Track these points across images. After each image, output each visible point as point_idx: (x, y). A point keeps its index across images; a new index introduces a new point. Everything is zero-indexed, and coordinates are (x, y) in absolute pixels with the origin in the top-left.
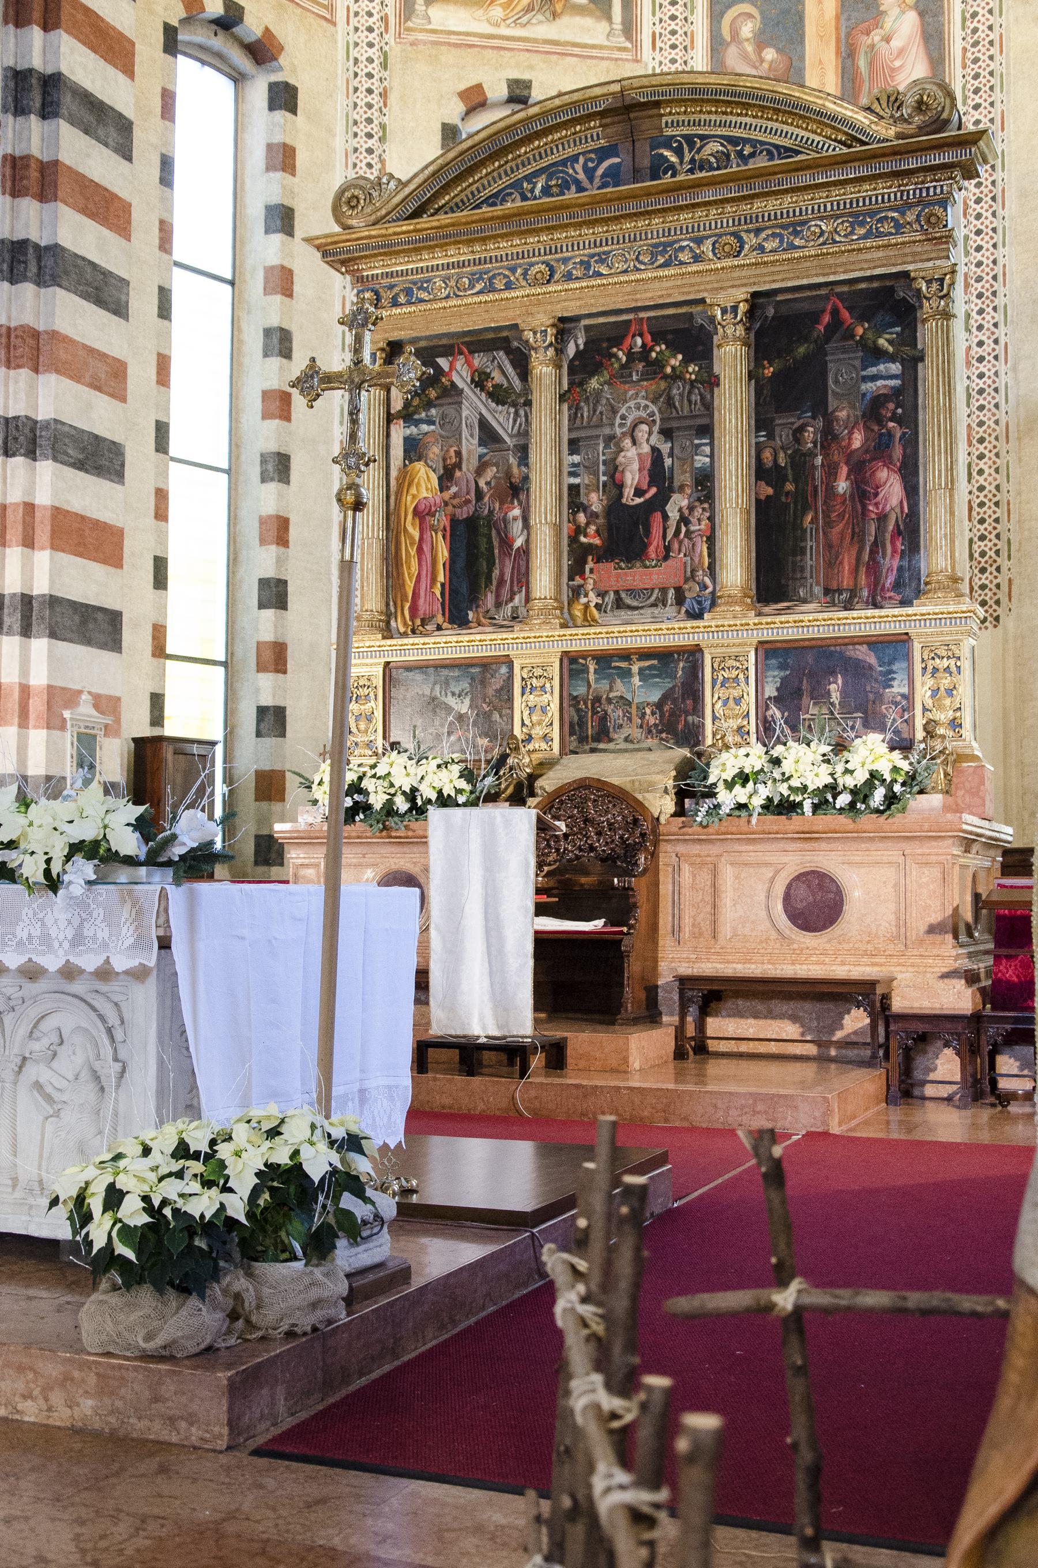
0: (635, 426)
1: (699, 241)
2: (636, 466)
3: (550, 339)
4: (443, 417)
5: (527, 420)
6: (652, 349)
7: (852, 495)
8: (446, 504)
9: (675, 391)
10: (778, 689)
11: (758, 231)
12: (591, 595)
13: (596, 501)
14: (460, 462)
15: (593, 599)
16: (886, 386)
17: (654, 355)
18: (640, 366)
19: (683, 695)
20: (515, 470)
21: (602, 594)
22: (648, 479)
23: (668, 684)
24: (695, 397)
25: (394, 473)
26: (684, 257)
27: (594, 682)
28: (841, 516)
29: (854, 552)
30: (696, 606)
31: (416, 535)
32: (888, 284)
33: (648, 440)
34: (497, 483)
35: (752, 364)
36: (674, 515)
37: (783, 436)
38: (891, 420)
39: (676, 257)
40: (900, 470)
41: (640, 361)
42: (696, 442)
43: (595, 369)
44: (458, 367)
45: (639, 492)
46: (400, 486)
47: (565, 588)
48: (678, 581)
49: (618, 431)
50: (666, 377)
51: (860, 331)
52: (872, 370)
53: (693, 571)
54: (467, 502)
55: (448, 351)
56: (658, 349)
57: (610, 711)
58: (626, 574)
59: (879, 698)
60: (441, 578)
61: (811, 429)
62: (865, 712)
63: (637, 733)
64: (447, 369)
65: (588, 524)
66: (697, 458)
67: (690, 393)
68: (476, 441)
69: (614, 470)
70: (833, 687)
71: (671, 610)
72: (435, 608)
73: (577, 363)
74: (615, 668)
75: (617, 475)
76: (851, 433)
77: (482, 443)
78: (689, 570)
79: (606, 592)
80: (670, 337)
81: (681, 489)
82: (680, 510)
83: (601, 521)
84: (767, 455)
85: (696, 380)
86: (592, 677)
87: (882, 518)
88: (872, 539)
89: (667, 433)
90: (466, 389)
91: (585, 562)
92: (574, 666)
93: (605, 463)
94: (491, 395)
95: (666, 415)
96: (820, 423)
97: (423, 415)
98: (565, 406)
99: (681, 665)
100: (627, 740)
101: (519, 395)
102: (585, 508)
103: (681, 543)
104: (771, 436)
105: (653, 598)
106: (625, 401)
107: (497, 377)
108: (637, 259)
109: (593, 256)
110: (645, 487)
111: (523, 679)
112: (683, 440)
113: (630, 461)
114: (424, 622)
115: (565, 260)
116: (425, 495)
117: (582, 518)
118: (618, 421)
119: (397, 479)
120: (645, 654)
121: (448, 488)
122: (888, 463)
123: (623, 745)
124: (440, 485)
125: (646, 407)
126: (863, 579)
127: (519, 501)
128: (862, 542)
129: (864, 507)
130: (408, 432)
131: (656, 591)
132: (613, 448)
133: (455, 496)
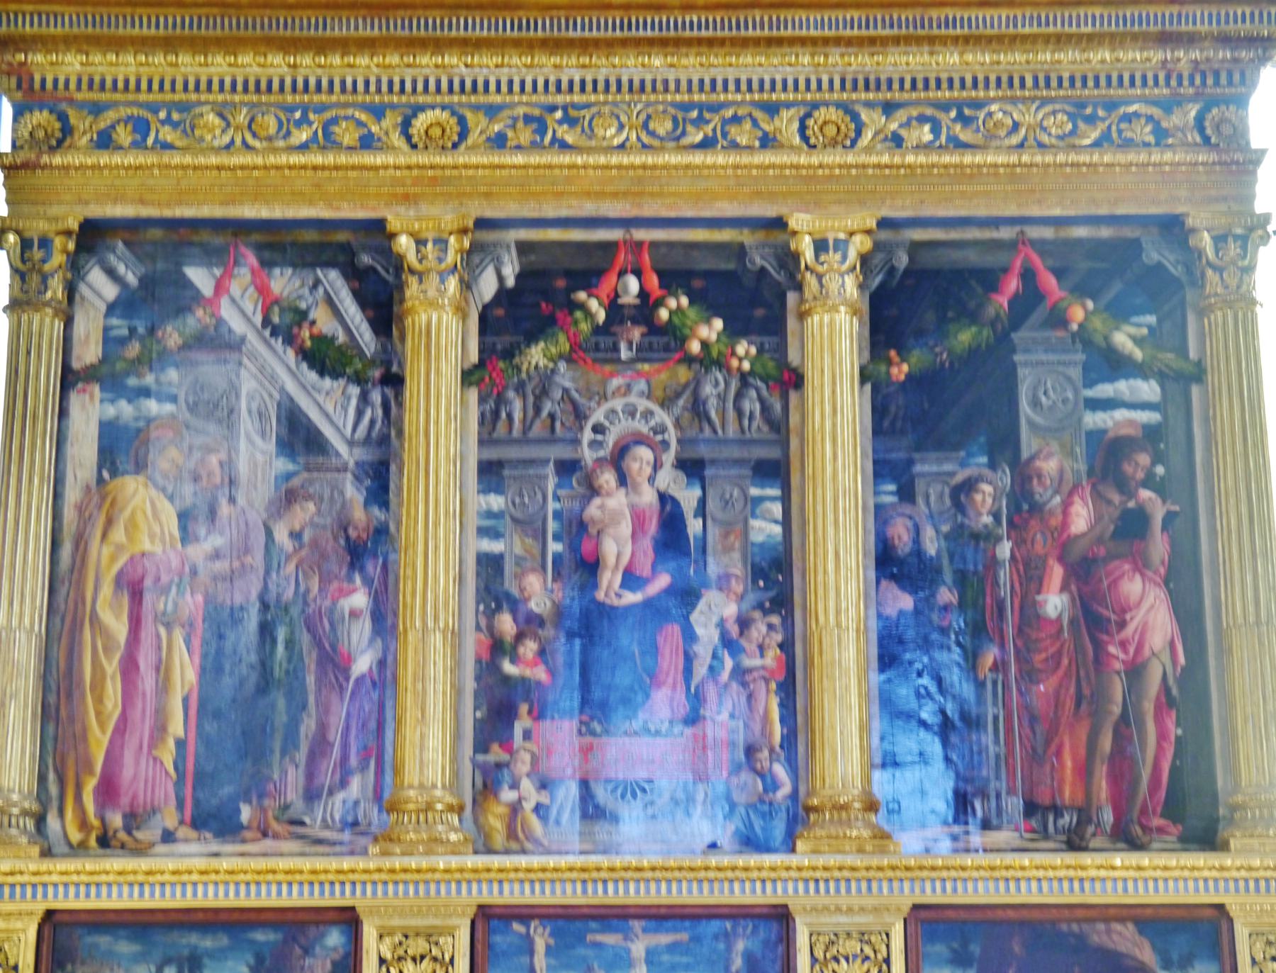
1: (772, 109)
2: (626, 528)
3: (451, 257)
6: (660, 303)
7: (1072, 621)
11: (889, 108)
12: (527, 785)
16: (1131, 423)
17: (664, 314)
18: (636, 333)
20: (359, 514)
24: (751, 404)
25: (72, 495)
26: (743, 135)
29: (1083, 733)
31: (119, 628)
32: (1129, 232)
33: (651, 480)
35: (867, 354)
39: (724, 135)
40: (1166, 583)
41: (635, 322)
42: (754, 491)
45: (631, 579)
47: (468, 766)
50: (689, 360)
51: (1077, 314)
52: (1105, 390)
55: (211, 256)
56: (672, 303)
60: (177, 727)
61: (987, 488)
65: (520, 637)
66: (755, 523)
67: (739, 396)
68: (271, 446)
72: (160, 794)
73: (500, 312)
76: (1067, 505)
80: (697, 284)
81: (723, 582)
82: (721, 624)
85: (752, 373)
87: (1135, 671)
88: (1117, 710)
89: (692, 468)
90: (252, 337)
93: (557, 515)
96: (1005, 478)
97: (149, 379)
98: (473, 395)
99: (740, 946)
102: (514, 604)
104: (907, 494)
106: (604, 397)
107: (324, 322)
108: (645, 126)
109: (552, 109)
113: (615, 518)
114: (133, 820)
115: (492, 111)
116: (147, 546)
117: (507, 624)
118: (588, 435)
119: (80, 509)
122: (1141, 565)
125: (648, 414)
126: (1102, 788)
128: (1097, 715)
129: (1099, 647)
130: (111, 411)
133: (216, 555)
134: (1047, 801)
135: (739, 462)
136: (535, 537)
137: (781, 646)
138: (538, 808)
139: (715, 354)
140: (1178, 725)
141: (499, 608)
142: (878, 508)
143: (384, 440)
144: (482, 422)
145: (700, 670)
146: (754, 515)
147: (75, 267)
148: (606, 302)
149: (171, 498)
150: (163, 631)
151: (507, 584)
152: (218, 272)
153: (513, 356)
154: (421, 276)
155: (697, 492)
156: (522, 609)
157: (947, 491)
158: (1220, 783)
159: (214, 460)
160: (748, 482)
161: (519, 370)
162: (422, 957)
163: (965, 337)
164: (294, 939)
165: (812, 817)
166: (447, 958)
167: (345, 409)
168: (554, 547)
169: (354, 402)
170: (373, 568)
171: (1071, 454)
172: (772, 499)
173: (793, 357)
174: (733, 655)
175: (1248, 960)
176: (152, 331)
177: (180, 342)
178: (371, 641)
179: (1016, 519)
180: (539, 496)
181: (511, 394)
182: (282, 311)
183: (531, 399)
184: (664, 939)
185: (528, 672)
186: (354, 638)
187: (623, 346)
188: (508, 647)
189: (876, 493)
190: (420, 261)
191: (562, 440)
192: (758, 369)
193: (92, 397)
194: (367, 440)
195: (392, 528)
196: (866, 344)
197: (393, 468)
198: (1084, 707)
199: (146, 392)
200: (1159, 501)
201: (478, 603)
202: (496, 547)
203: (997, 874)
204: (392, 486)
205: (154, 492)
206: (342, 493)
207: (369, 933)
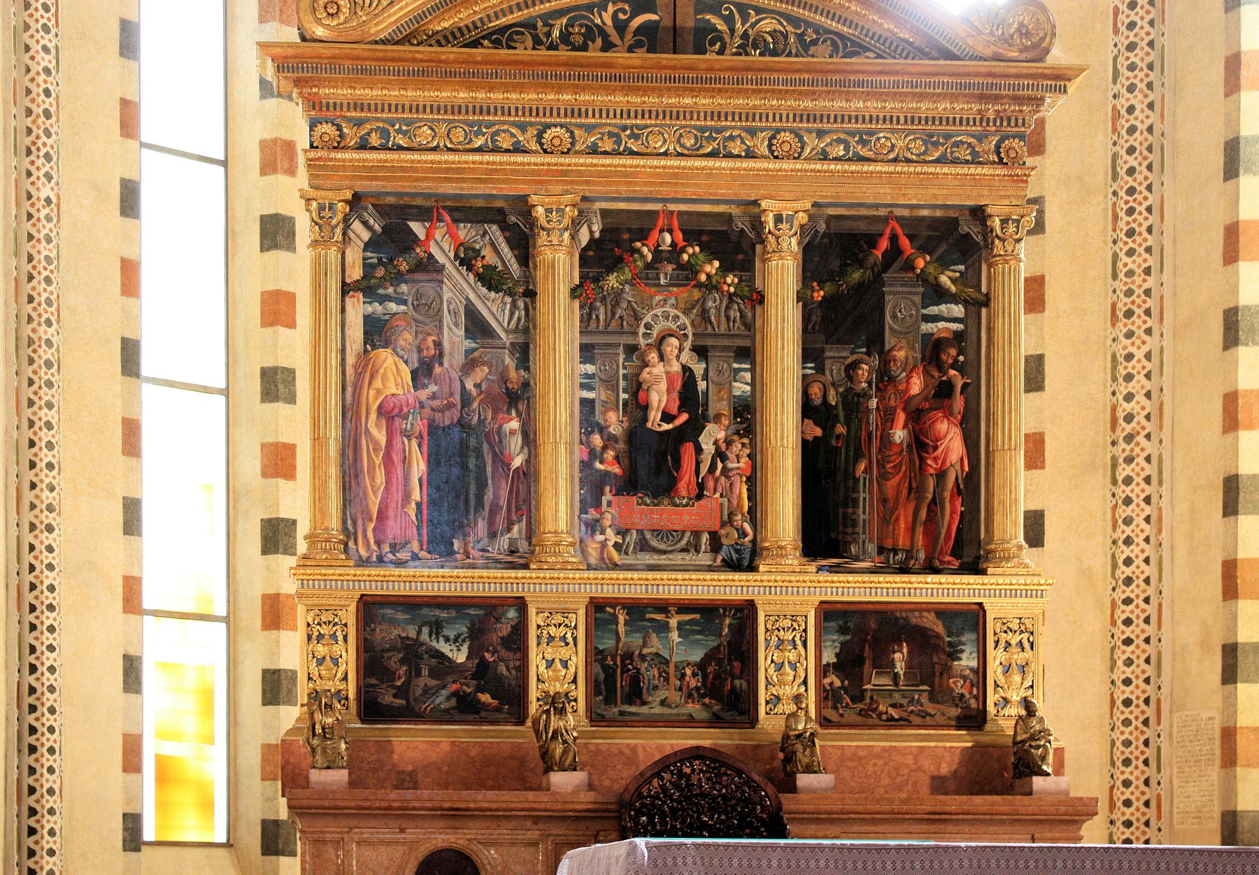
0: (662, 339)
2: (663, 386)
3: (567, 221)
4: (418, 296)
5: (527, 314)
8: (422, 406)
9: (710, 304)
10: (837, 655)
12: (609, 532)
13: (615, 423)
14: (441, 355)
15: (612, 537)
18: (670, 268)
19: (730, 654)
20: (513, 374)
21: (622, 533)
22: (677, 403)
23: (713, 642)
25: (351, 360)
27: (625, 634)
28: (897, 467)
30: (734, 556)
33: (678, 357)
34: (489, 388)
36: (708, 448)
37: (834, 370)
38: (953, 367)
40: (961, 424)
41: (670, 262)
42: (736, 366)
43: (615, 264)
44: (438, 236)
45: (667, 417)
46: (359, 375)
48: (714, 524)
49: (642, 342)
50: (700, 285)
53: (731, 515)
54: (450, 406)
55: (424, 214)
57: (643, 670)
58: (652, 513)
59: (947, 670)
61: (866, 367)
62: (931, 685)
63: (676, 697)
64: (422, 237)
65: (604, 448)
67: (728, 308)
68: (462, 332)
69: (637, 387)
70: (897, 656)
71: (704, 558)
72: (409, 532)
73: (591, 253)
74: (652, 620)
75: (641, 395)
76: (909, 378)
77: (469, 334)
78: (726, 512)
79: (628, 530)
81: (717, 418)
82: (716, 443)
83: (621, 446)
84: (816, 390)
86: (621, 628)
87: (941, 475)
88: (930, 496)
89: (701, 352)
90: (448, 265)
91: (602, 493)
92: (598, 615)
94: (480, 278)
95: (700, 330)
97: (391, 290)
98: (577, 304)
99: (727, 621)
100: (663, 703)
101: (517, 283)
102: (602, 430)
103: (716, 480)
104: (820, 369)
105: (684, 542)
107: (490, 257)
110: (674, 411)
111: (539, 627)
112: (720, 363)
116: (394, 391)
117: (597, 440)
118: (642, 330)
120: (685, 607)
121: (424, 386)
122: (949, 414)
123: (658, 710)
124: (413, 379)
125: (676, 318)
126: (920, 539)
127: (517, 411)
128: (919, 500)
129: (922, 460)
130: (370, 309)
131: (688, 534)
132: (638, 363)
133: (434, 396)
134: (890, 547)
135: (726, 348)
136: (613, 391)
137: (749, 456)
138: (616, 545)
139: (714, 282)
140: (962, 506)
141: (592, 432)
142: (804, 376)
143: (526, 331)
144: (581, 321)
145: (704, 469)
146: (736, 381)
147: (346, 220)
148: (652, 248)
149: (406, 362)
150: (405, 440)
151: (597, 417)
152: (427, 225)
153: (599, 281)
154: (549, 231)
155: (704, 366)
156: (605, 432)
157: (843, 367)
158: (982, 537)
159: (430, 339)
160: (732, 360)
161: (603, 289)
162: (560, 625)
163: (856, 276)
164: (491, 614)
165: (765, 553)
166: (573, 624)
167: (503, 311)
168: (623, 396)
169: (508, 306)
170: (522, 407)
171: (913, 348)
172: (746, 370)
173: (758, 284)
174: (722, 462)
175: (992, 633)
176: (391, 260)
177: (407, 267)
178: (522, 448)
179: (881, 385)
180: (615, 366)
181: (598, 304)
182: (466, 250)
183: (610, 307)
184: (687, 617)
185: (609, 469)
186: (513, 446)
187: (662, 276)
188: (598, 454)
189: (803, 368)
190: (548, 222)
191: (626, 333)
192: (739, 292)
193: (358, 300)
194: (516, 330)
195: (532, 382)
196: (800, 278)
197: (531, 346)
198: (912, 495)
199: (389, 298)
200: (960, 377)
201: (581, 428)
202: (590, 395)
203: (866, 585)
204: (531, 358)
205: (397, 358)
206: (503, 361)
207: (532, 611)
